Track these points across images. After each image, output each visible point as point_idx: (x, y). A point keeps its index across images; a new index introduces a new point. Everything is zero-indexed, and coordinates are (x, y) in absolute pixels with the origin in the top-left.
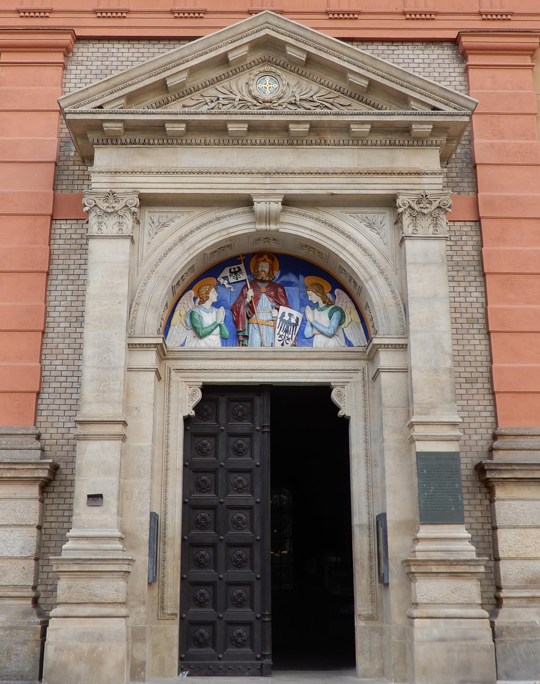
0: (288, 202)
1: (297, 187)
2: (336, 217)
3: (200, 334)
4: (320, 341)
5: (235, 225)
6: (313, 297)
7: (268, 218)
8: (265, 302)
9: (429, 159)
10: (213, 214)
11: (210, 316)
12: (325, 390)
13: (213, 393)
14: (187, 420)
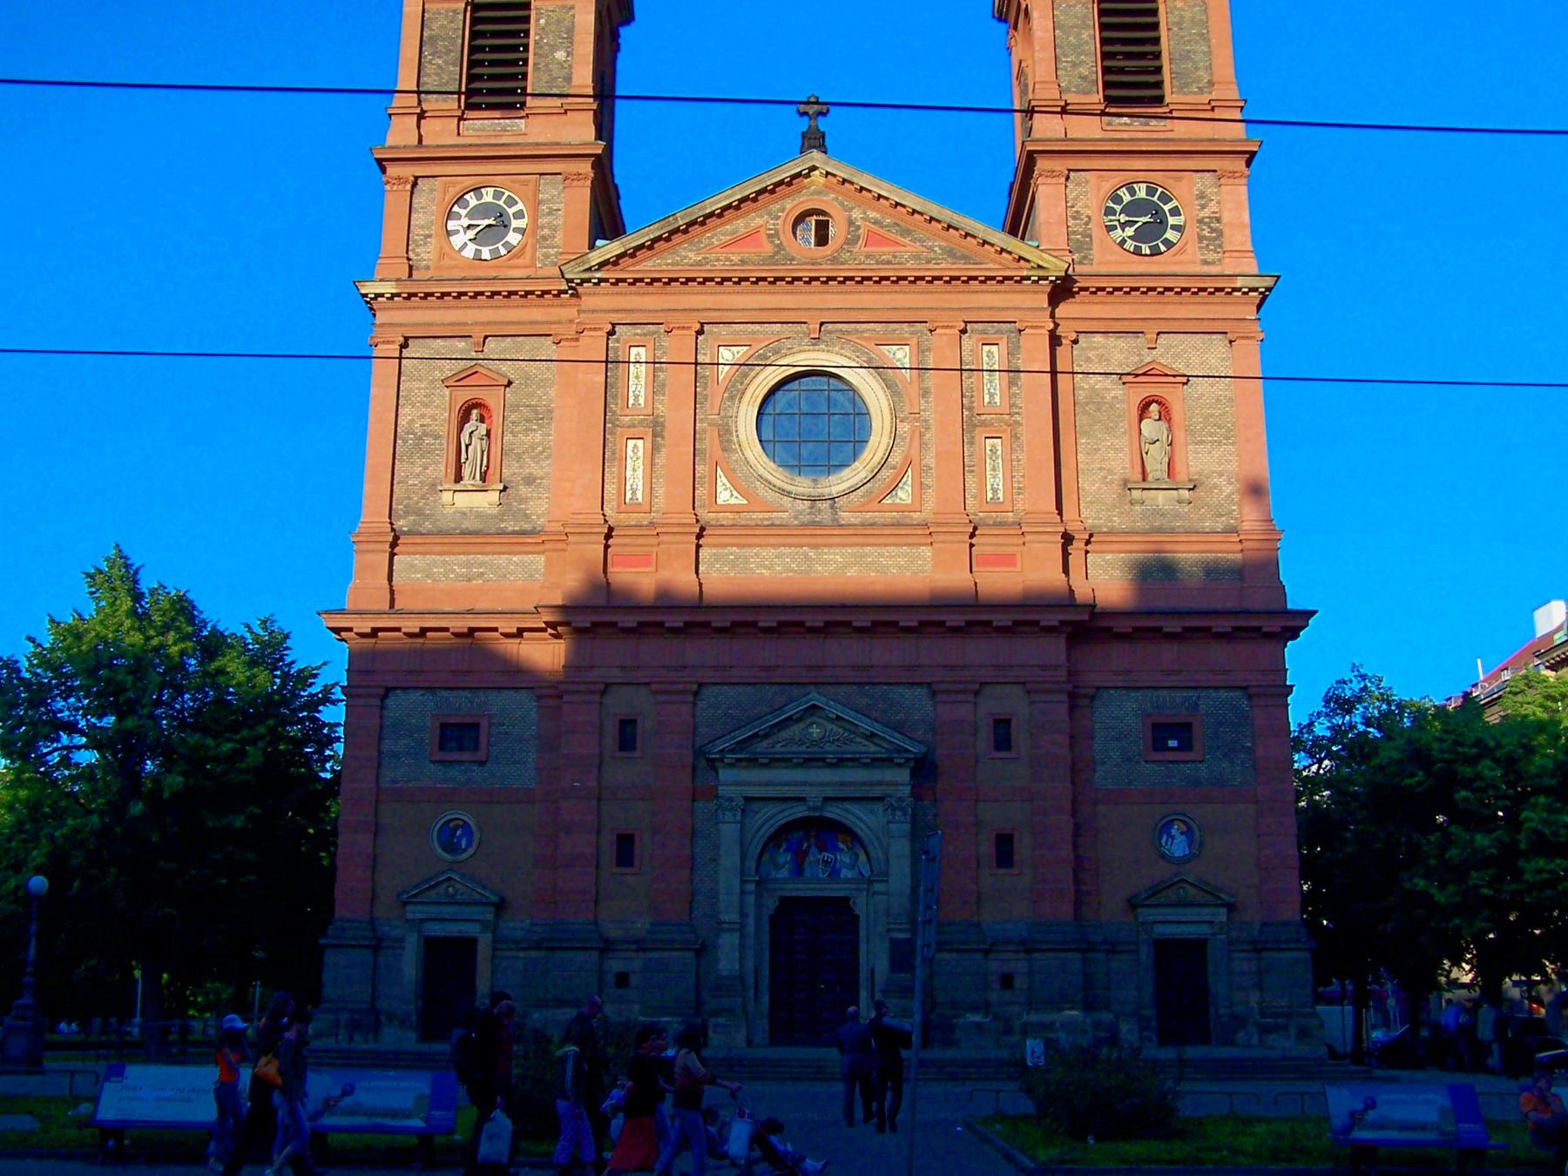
0: (826, 799)
1: (830, 792)
2: (855, 808)
3: (778, 867)
4: (846, 873)
5: (800, 811)
6: (841, 846)
7: (815, 808)
8: (814, 850)
9: (904, 775)
10: (783, 806)
11: (784, 857)
12: (846, 899)
13: (785, 902)
14: (771, 917)
